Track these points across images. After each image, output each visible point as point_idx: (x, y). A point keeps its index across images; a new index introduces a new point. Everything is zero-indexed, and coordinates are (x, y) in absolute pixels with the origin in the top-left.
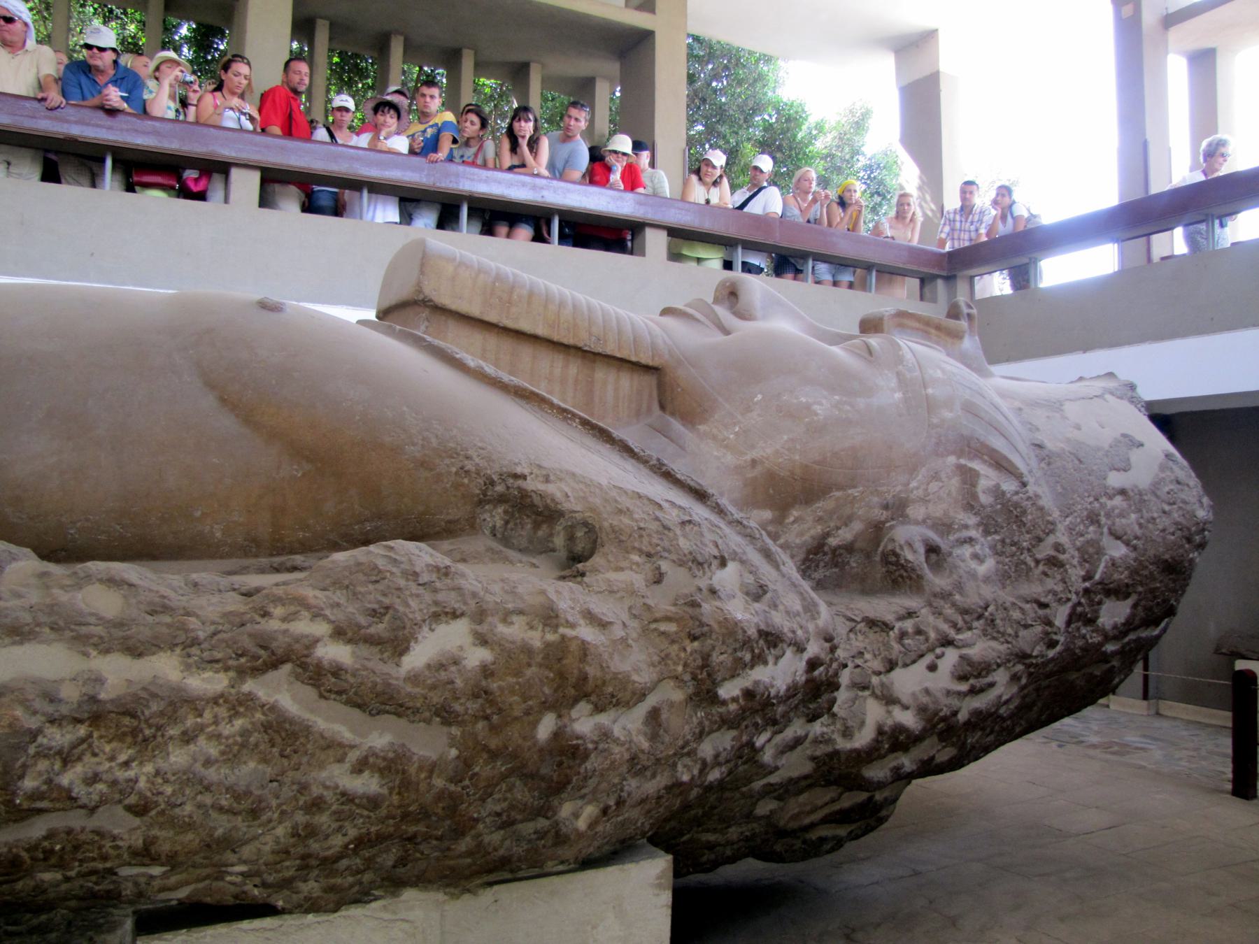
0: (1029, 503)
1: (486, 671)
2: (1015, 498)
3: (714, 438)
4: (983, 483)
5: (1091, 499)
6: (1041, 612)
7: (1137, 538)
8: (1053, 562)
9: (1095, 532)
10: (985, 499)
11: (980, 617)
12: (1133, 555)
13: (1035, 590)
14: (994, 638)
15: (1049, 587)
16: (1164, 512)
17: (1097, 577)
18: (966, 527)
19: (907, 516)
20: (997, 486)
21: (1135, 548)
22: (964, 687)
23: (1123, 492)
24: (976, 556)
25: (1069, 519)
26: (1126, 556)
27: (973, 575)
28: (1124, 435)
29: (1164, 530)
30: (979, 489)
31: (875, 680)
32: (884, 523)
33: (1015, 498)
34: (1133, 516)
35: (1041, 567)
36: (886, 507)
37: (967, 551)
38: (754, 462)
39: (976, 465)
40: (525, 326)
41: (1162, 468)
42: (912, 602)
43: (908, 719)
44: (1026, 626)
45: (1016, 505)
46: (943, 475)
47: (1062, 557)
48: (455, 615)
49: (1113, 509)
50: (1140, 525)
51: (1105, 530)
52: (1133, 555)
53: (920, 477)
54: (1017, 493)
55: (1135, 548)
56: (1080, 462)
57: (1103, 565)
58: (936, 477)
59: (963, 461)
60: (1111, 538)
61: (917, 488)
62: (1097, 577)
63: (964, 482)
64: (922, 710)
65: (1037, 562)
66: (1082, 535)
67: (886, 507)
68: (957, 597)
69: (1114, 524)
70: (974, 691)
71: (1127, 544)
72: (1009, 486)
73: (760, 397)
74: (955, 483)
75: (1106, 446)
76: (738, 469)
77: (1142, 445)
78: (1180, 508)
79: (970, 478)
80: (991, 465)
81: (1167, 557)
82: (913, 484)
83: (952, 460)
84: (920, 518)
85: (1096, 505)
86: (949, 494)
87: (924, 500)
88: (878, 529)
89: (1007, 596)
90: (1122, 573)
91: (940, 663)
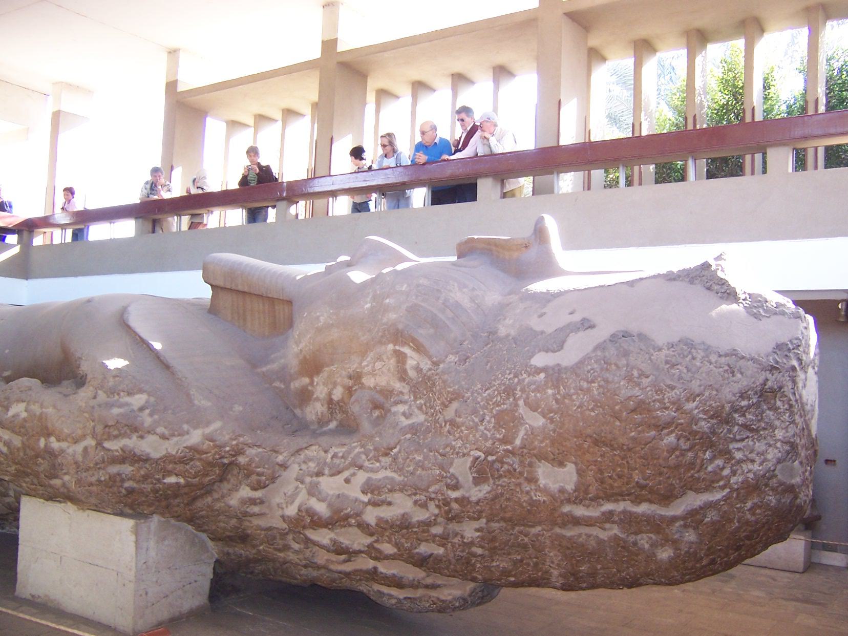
0: (437, 377)
1: (25, 420)
4: (410, 363)
5: (512, 376)
7: (551, 411)
10: (412, 374)
11: (386, 454)
12: (552, 427)
17: (518, 442)
18: (401, 393)
19: (363, 384)
21: (552, 420)
22: (365, 499)
23: (544, 369)
26: (544, 426)
30: (408, 367)
32: (351, 387)
34: (550, 392)
39: (406, 350)
40: (240, 288)
41: (596, 348)
43: (321, 508)
46: (384, 357)
48: (23, 401)
50: (557, 401)
51: (521, 403)
52: (552, 427)
53: (369, 359)
54: (430, 369)
57: (522, 433)
58: (379, 358)
59: (397, 348)
60: (527, 409)
61: (367, 366)
62: (518, 442)
63: (398, 362)
66: (498, 406)
67: (350, 377)
68: (377, 439)
70: (375, 504)
74: (393, 361)
79: (401, 358)
80: (414, 350)
81: (589, 431)
82: (364, 363)
83: (391, 347)
84: (372, 386)
86: (389, 370)
87: (373, 373)
90: (542, 442)
91: (352, 479)
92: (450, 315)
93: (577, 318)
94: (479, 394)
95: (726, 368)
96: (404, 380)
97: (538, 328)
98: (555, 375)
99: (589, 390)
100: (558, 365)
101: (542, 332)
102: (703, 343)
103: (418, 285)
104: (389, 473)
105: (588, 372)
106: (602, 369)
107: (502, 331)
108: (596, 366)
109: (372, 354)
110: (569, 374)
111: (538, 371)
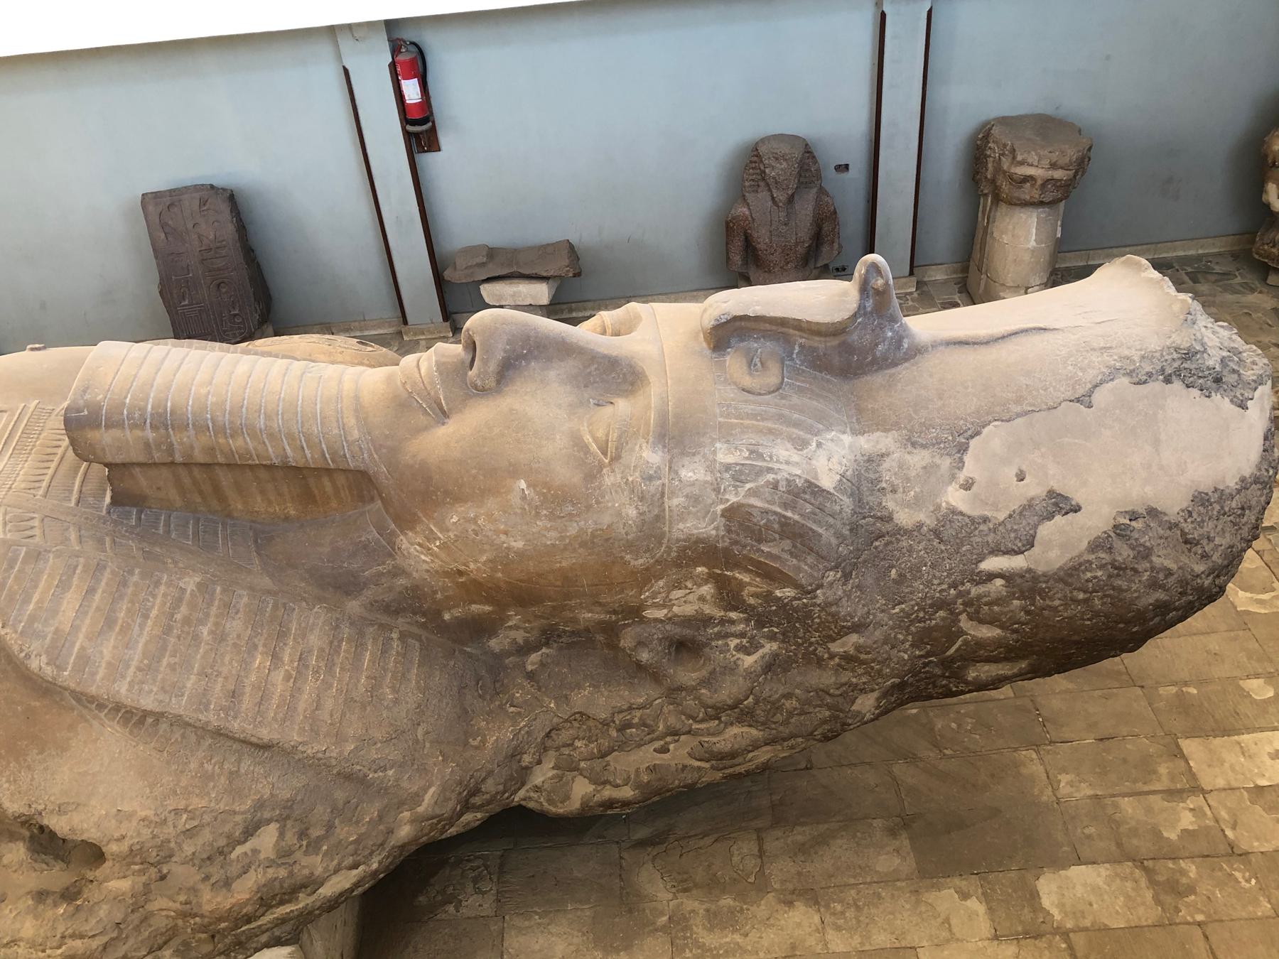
2: (795, 603)
3: (420, 545)
6: (829, 700)
8: (847, 658)
9: (943, 619)
12: (1015, 636)
13: (826, 679)
14: (750, 726)
15: (844, 680)
16: (1074, 600)
18: (732, 622)
20: (770, 593)
22: (707, 765)
24: (739, 648)
25: (897, 610)
27: (731, 669)
28: (1052, 494)
29: (1070, 618)
31: (583, 764)
33: (795, 603)
34: (1016, 602)
35: (837, 660)
36: (615, 612)
37: (733, 643)
38: (460, 573)
41: (1095, 546)
42: (645, 693)
43: (627, 793)
44: (803, 713)
45: (796, 610)
46: (689, 585)
47: (863, 656)
49: (979, 597)
50: (1028, 613)
54: (795, 599)
55: (1016, 631)
56: (941, 541)
62: (948, 653)
64: (638, 786)
65: (832, 657)
69: (977, 612)
71: (1002, 627)
72: (786, 593)
73: (455, 519)
74: (707, 590)
75: (1002, 516)
76: (447, 574)
77: (1077, 509)
78: (1105, 596)
80: (759, 575)
85: (952, 591)
88: (611, 631)
89: (773, 689)
92: (809, 508)
93: (1034, 489)
94: (883, 611)
96: (735, 609)
97: (975, 513)
98: (1026, 585)
99: (1086, 601)
100: (1029, 570)
101: (985, 520)
102: (1216, 490)
103: (728, 467)
104: (735, 730)
105: (1088, 581)
106: (1110, 576)
107: (904, 518)
108: (1099, 573)
109: (661, 583)
110: (1052, 582)
111: (991, 576)
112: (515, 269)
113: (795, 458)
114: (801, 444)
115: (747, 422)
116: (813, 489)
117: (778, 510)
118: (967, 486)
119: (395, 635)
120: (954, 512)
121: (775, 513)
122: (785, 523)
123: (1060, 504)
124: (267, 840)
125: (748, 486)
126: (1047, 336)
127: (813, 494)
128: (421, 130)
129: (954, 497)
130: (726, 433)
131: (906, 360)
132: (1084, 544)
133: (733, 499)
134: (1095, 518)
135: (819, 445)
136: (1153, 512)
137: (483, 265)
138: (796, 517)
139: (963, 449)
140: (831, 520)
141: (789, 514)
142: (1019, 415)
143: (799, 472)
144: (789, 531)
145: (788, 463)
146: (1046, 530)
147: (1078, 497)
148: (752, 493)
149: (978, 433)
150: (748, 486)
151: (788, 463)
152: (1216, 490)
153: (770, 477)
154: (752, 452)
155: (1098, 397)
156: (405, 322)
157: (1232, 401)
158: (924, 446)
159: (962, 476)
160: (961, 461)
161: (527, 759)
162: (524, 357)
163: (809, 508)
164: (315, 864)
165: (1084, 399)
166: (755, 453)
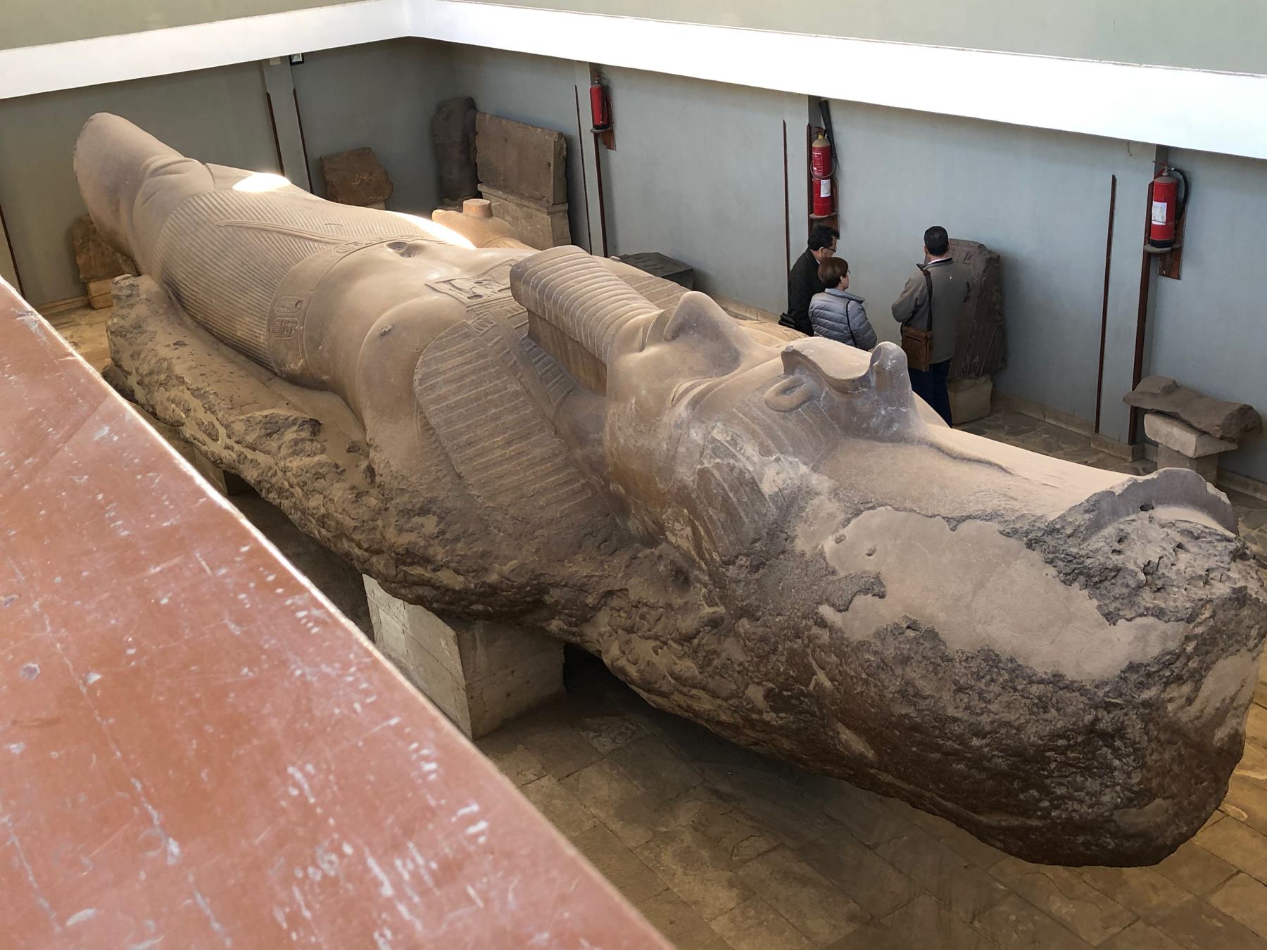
74: (688, 530)
75: (842, 574)
92: (745, 499)
93: (870, 565)
95: (1036, 701)
97: (832, 563)
102: (1012, 660)
103: (714, 440)
106: (878, 666)
112: (1178, 411)
113: (756, 459)
114: (765, 452)
115: (746, 420)
116: (754, 486)
117: (726, 487)
118: (839, 541)
119: (582, 481)
120: (822, 554)
121: (723, 489)
122: (726, 499)
123: (875, 588)
124: (430, 524)
125: (718, 460)
126: (1001, 474)
127: (752, 489)
128: (1165, 251)
129: (828, 545)
130: (729, 420)
131: (892, 441)
132: (873, 630)
133: (706, 465)
134: (887, 612)
135: (778, 460)
136: (932, 635)
137: (1154, 395)
138: (735, 500)
139: (857, 513)
140: (756, 517)
141: (731, 495)
142: (905, 510)
143: (751, 469)
144: (729, 510)
145: (748, 458)
146: (861, 601)
147: (890, 589)
148: (718, 466)
149: (873, 508)
150: (718, 460)
151: (748, 458)
152: (1012, 660)
153: (732, 461)
154: (733, 439)
155: (964, 527)
156: (1097, 430)
157: (1099, 607)
158: (839, 500)
159: (842, 532)
160: (848, 521)
161: (590, 600)
162: (692, 328)
163: (745, 499)
164: (439, 554)
165: (955, 522)
166: (734, 442)
